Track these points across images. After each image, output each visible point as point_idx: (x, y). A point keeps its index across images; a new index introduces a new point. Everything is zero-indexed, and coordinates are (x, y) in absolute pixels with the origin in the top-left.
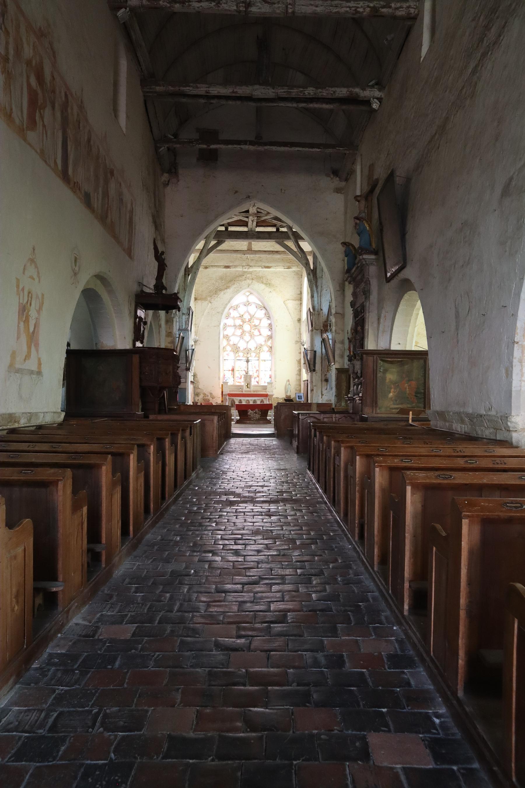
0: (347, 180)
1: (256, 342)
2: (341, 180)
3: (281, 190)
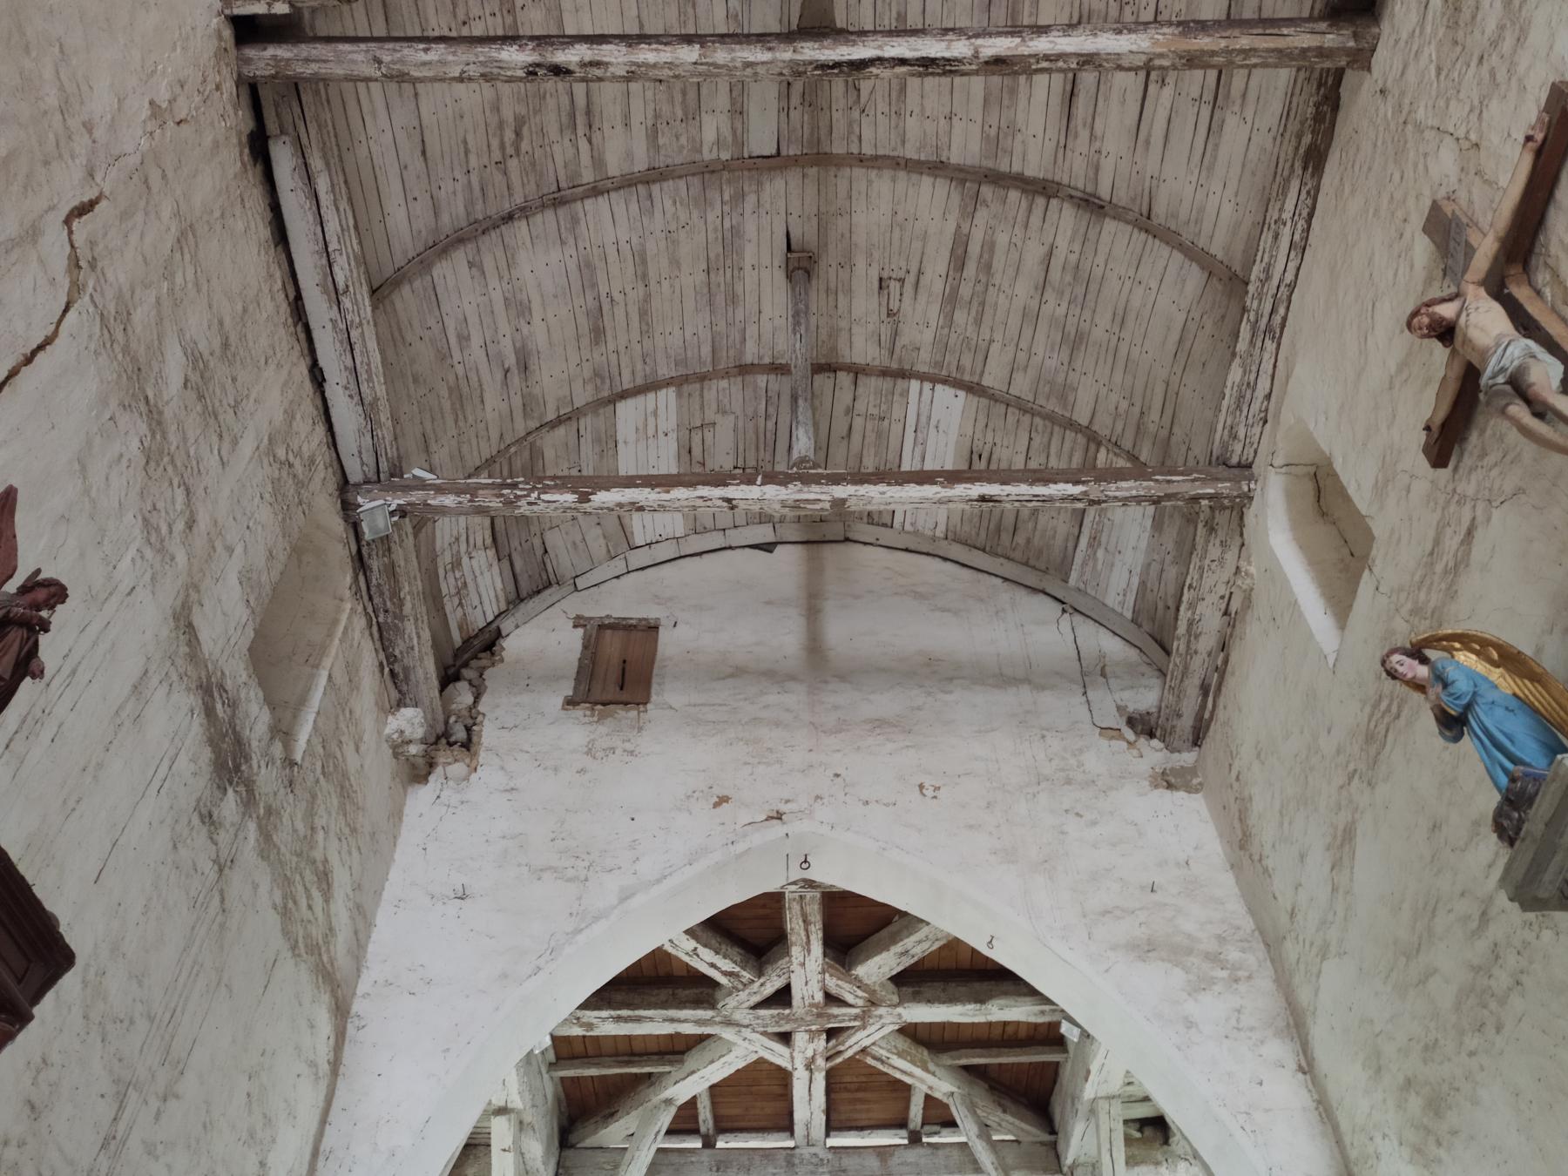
0: (1198, 737)
2: (1171, 748)
3: (921, 787)
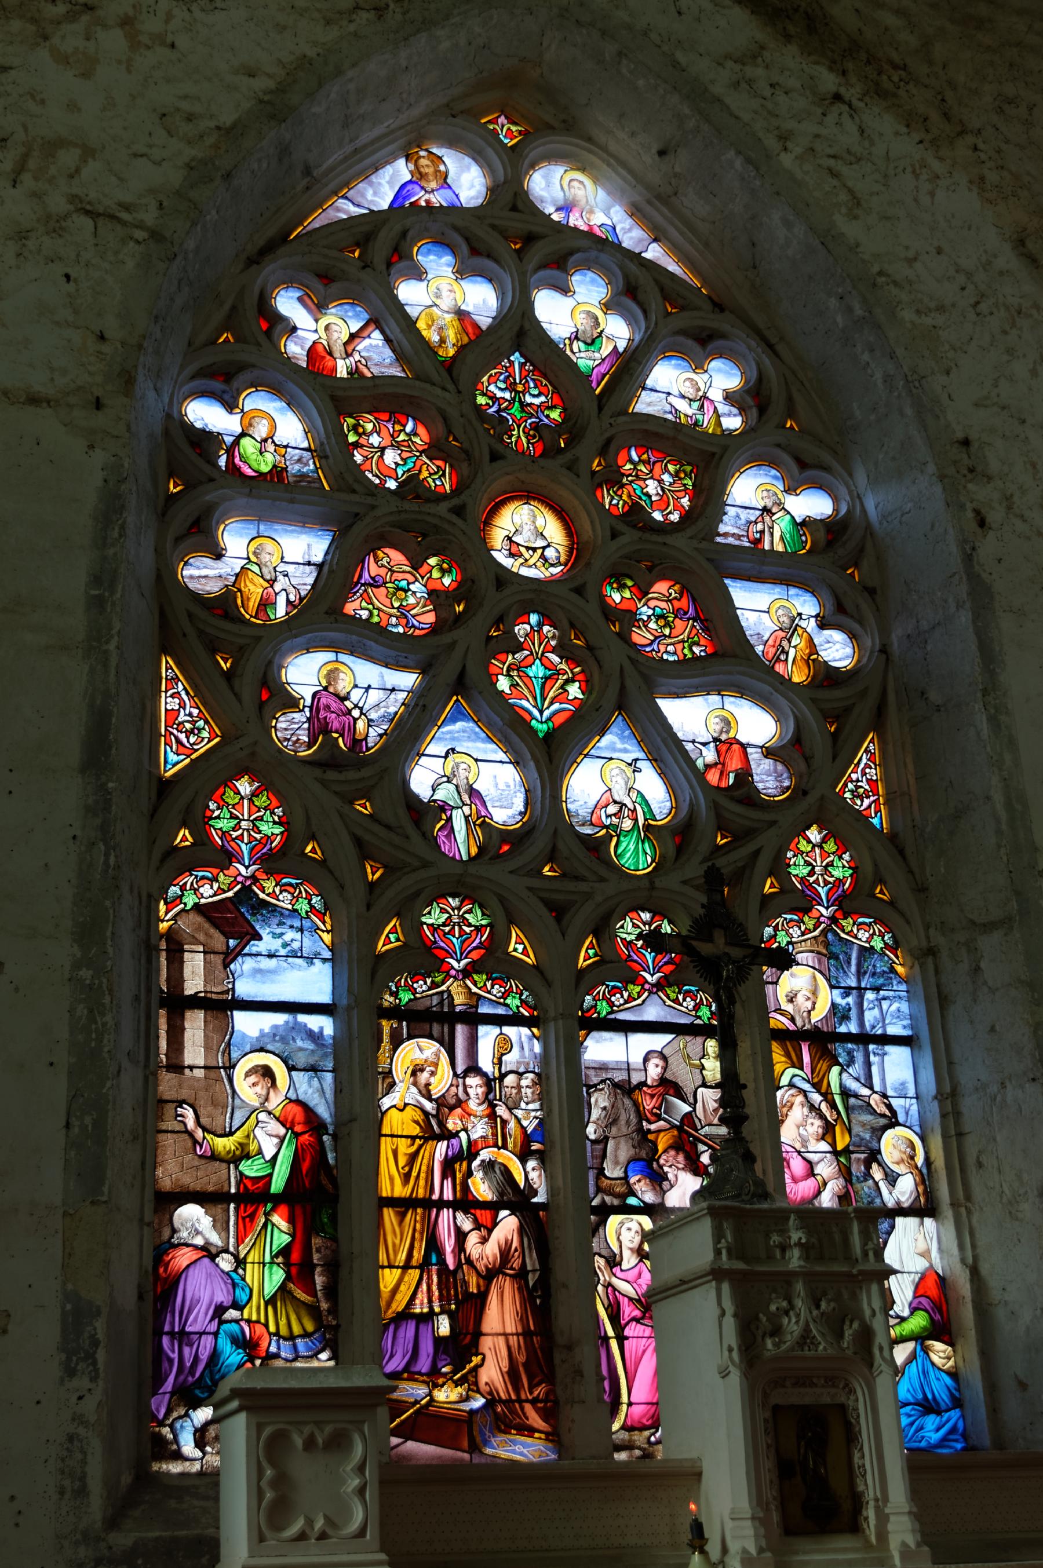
1: (663, 747)
